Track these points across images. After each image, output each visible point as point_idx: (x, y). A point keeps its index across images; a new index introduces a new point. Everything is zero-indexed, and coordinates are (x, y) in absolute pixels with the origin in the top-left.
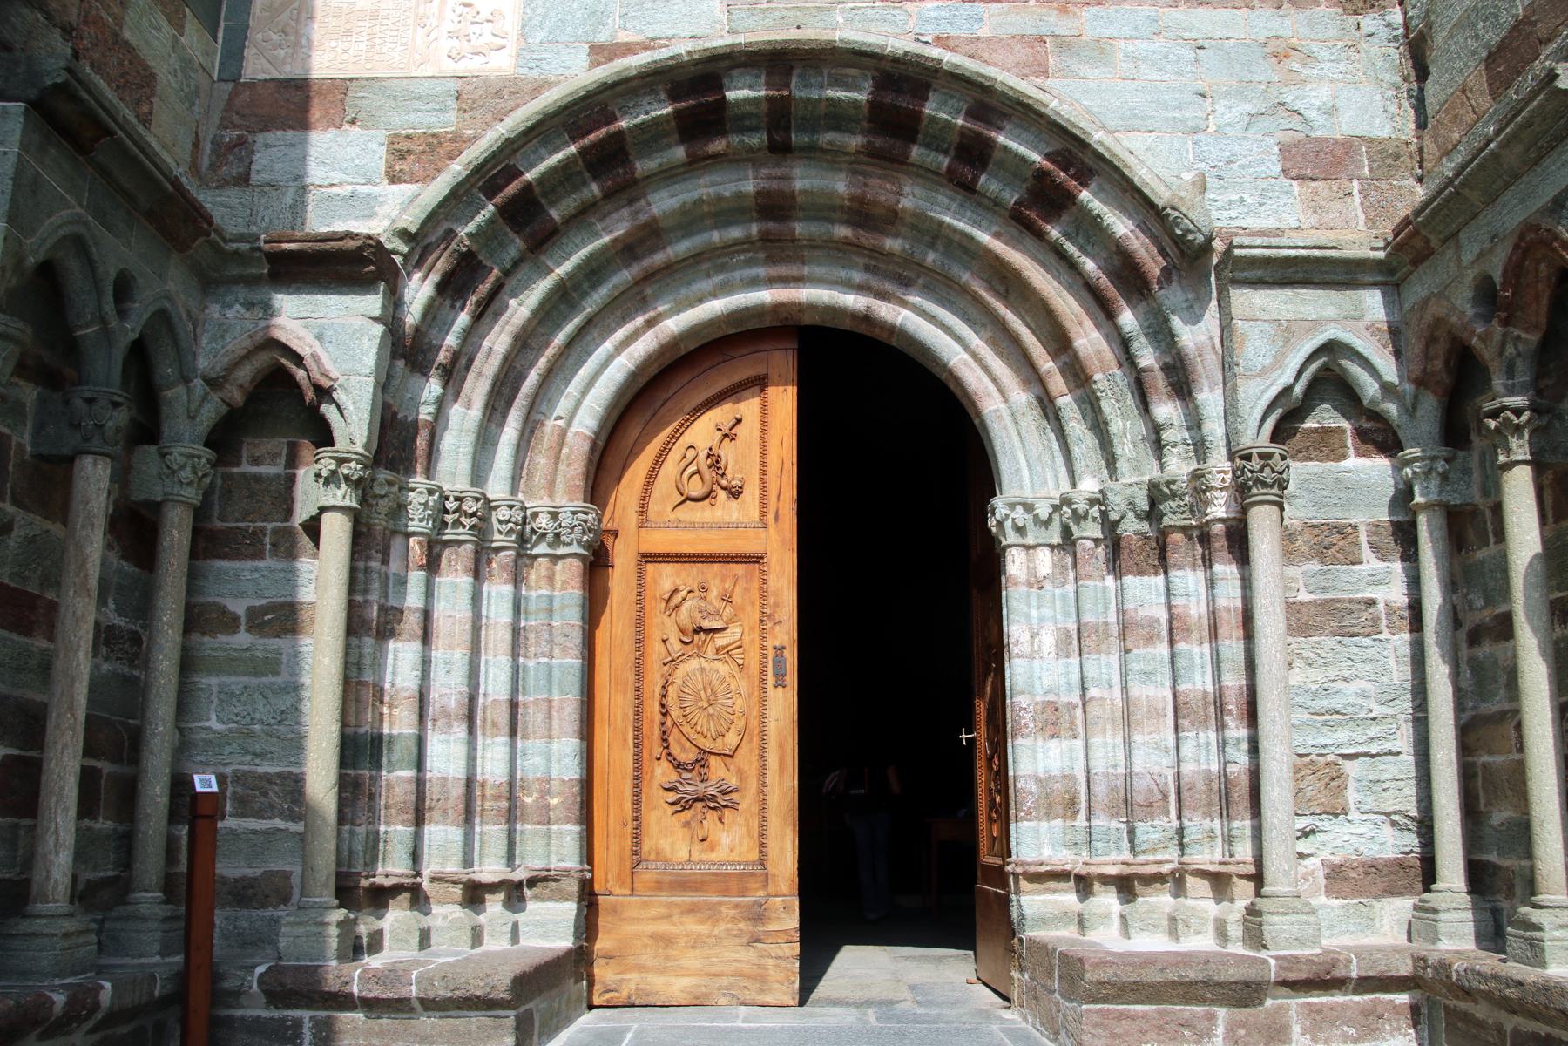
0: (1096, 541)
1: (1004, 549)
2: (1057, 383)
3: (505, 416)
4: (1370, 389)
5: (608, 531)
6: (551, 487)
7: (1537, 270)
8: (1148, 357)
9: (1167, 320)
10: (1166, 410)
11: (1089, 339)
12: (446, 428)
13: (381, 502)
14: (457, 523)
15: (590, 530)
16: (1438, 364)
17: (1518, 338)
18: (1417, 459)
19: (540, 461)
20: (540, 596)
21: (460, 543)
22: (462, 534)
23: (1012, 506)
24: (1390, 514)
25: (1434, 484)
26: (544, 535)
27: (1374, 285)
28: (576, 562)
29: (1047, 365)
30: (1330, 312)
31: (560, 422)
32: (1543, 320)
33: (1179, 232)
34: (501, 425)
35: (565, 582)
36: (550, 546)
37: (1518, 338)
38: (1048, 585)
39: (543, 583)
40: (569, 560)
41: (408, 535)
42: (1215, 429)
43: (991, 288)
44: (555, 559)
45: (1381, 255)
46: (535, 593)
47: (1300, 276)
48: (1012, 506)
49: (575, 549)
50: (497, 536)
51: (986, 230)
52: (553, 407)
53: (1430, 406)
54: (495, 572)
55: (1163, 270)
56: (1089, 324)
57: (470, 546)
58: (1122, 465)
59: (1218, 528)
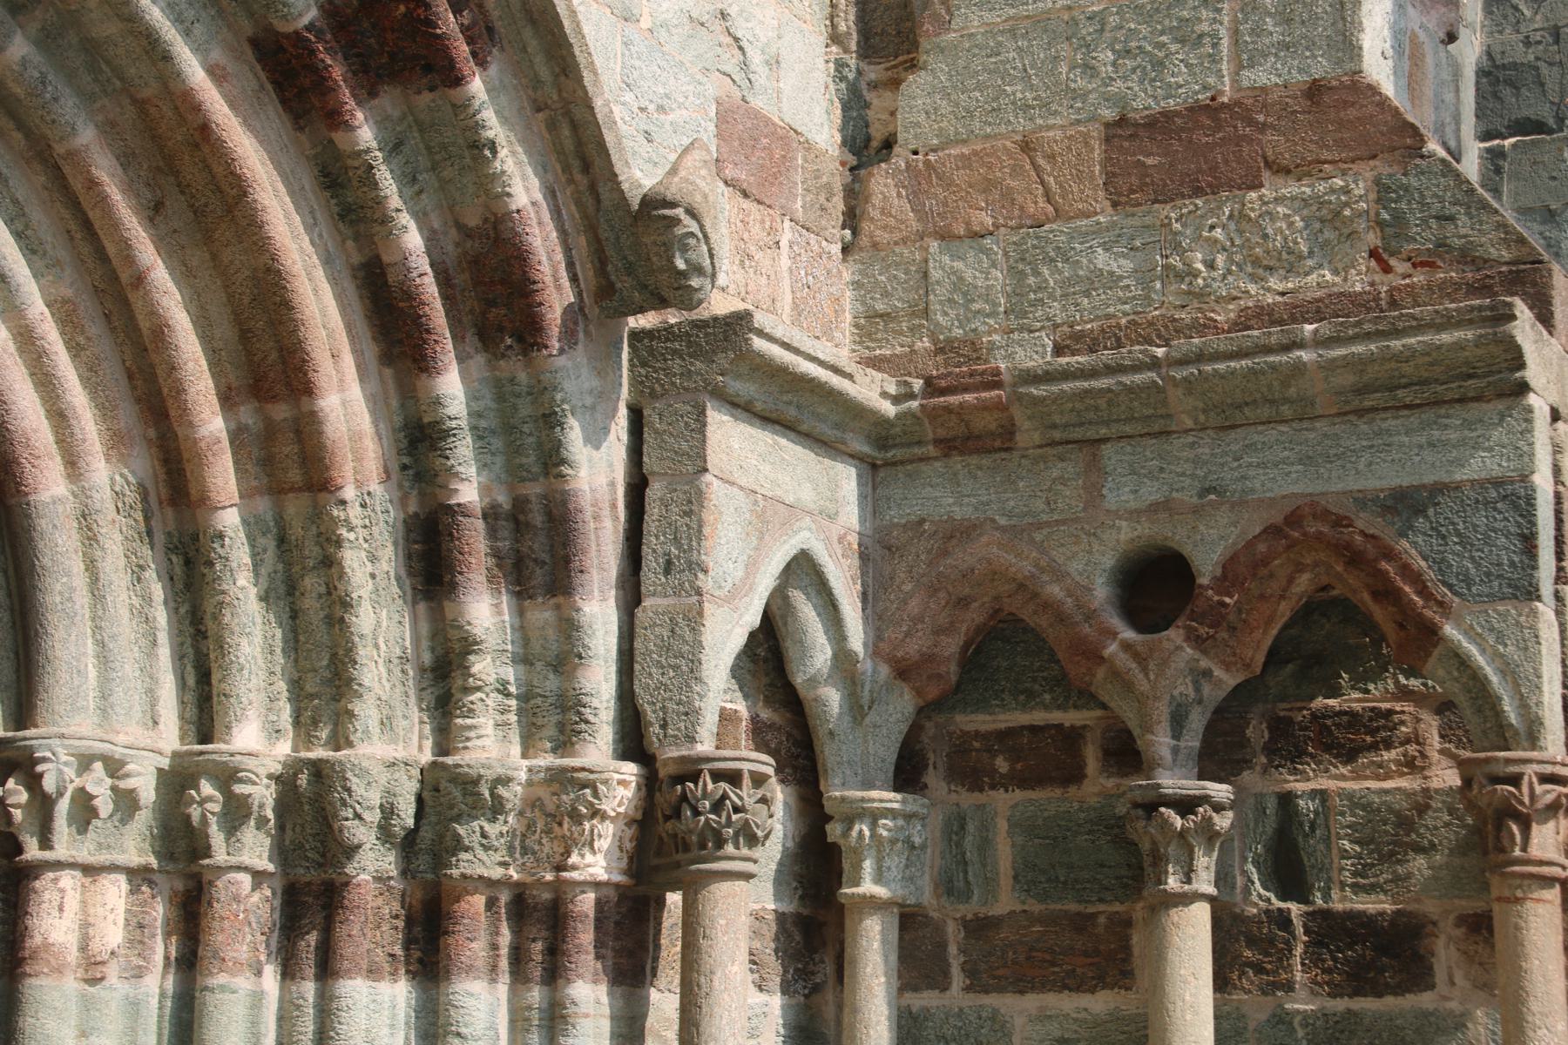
0: (258, 876)
1: (33, 871)
2: (223, 477)
4: (815, 654)
7: (1291, 580)
8: (469, 490)
9: (551, 421)
10: (485, 611)
11: (347, 404)
16: (951, 646)
17: (1207, 673)
18: (892, 814)
23: (85, 762)
24: (778, 897)
25: (894, 863)
27: (855, 457)
29: (211, 423)
30: (807, 495)
32: (1260, 658)
33: (680, 264)
37: (1207, 673)
38: (112, 971)
42: (599, 682)
43: (129, 189)
45: (889, 409)
47: (792, 412)
48: (85, 762)
51: (197, 50)
53: (899, 709)
55: (568, 310)
56: (348, 361)
58: (367, 712)
59: (586, 902)
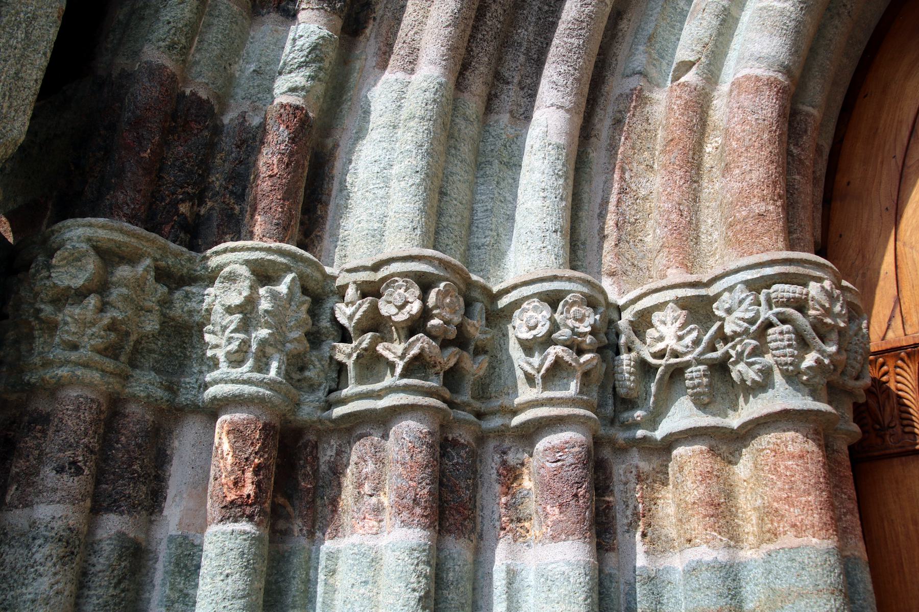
3: (531, 93)
5: (893, 351)
6: (687, 237)
12: (360, 134)
13: (73, 312)
14: (371, 364)
15: (822, 331)
19: (652, 182)
20: (693, 570)
21: (383, 420)
22: (391, 391)
26: (676, 373)
28: (793, 441)
31: (690, 77)
34: (525, 116)
35: (768, 513)
36: (702, 405)
39: (696, 525)
40: (767, 440)
41: (213, 410)
44: (727, 443)
46: (676, 553)
49: (781, 397)
50: (526, 393)
52: (664, 54)
54: (531, 506)
57: (408, 429)
